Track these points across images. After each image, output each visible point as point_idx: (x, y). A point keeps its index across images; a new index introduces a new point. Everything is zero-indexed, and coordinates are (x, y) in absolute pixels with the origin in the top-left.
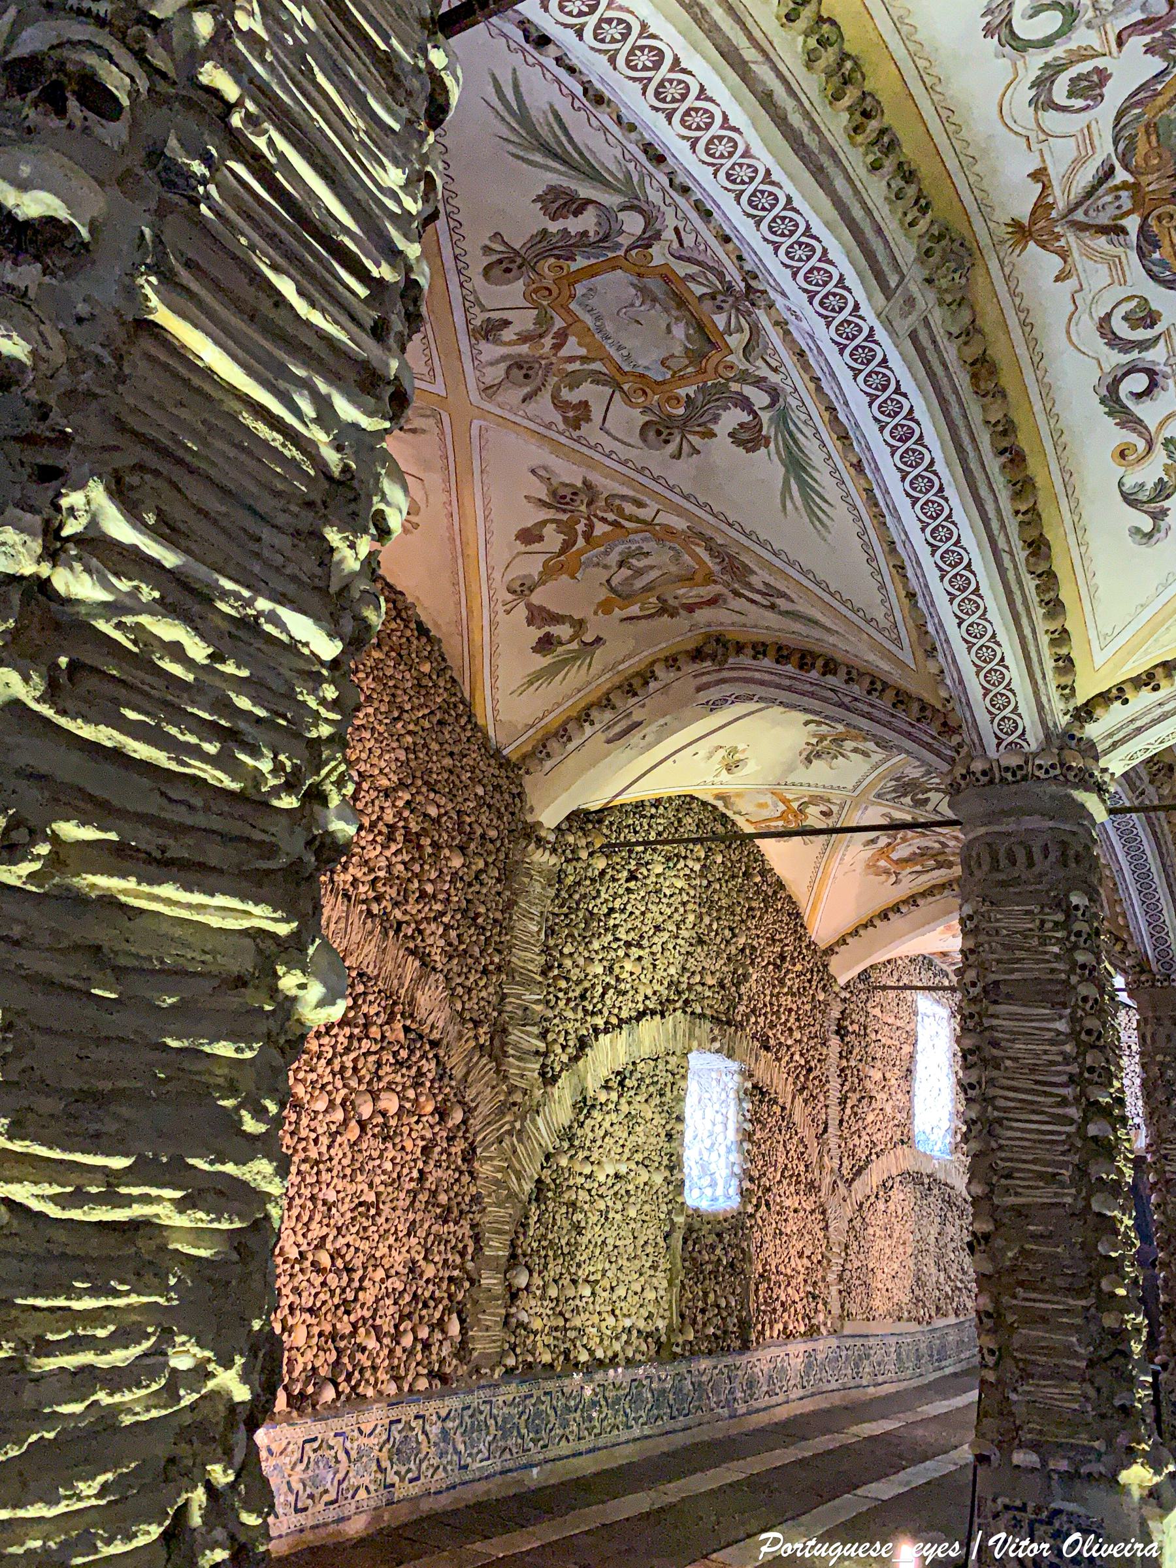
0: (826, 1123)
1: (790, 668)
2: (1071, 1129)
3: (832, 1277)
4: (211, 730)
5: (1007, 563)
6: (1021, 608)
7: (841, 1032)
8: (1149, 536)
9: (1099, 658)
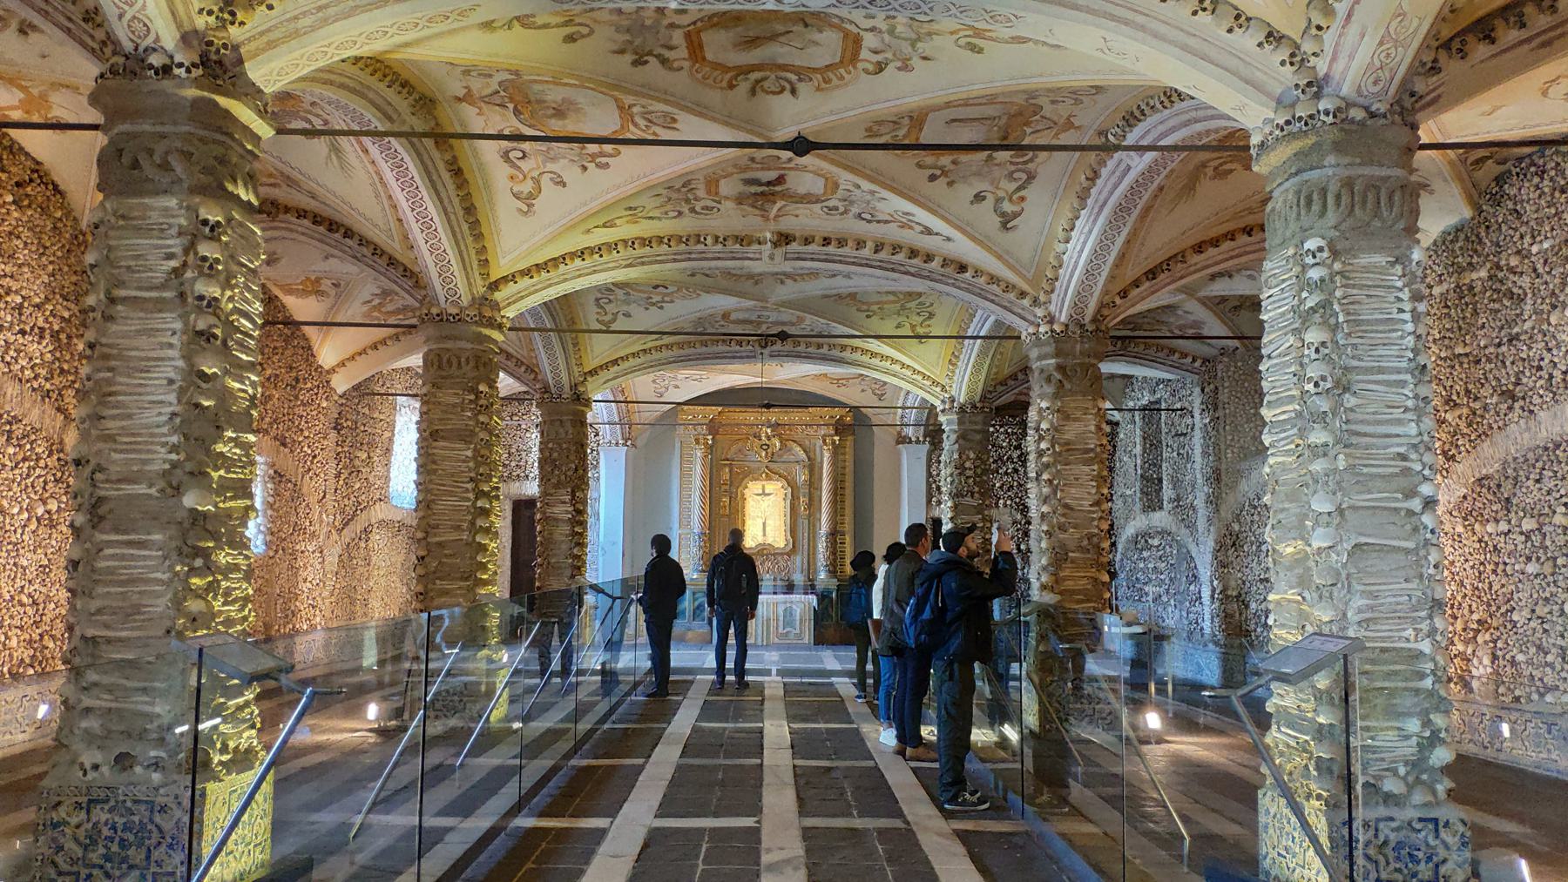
0: (325, 492)
1: (321, 229)
2: (469, 504)
3: (326, 594)
4: (240, 467)
5: (453, 217)
6: (459, 237)
7: (337, 427)
8: (526, 213)
9: (502, 262)
